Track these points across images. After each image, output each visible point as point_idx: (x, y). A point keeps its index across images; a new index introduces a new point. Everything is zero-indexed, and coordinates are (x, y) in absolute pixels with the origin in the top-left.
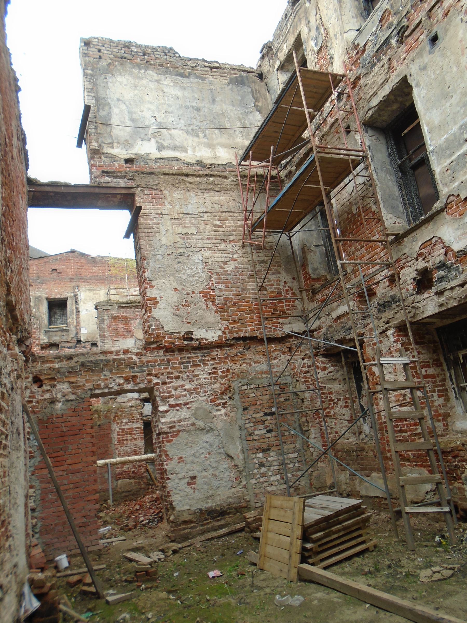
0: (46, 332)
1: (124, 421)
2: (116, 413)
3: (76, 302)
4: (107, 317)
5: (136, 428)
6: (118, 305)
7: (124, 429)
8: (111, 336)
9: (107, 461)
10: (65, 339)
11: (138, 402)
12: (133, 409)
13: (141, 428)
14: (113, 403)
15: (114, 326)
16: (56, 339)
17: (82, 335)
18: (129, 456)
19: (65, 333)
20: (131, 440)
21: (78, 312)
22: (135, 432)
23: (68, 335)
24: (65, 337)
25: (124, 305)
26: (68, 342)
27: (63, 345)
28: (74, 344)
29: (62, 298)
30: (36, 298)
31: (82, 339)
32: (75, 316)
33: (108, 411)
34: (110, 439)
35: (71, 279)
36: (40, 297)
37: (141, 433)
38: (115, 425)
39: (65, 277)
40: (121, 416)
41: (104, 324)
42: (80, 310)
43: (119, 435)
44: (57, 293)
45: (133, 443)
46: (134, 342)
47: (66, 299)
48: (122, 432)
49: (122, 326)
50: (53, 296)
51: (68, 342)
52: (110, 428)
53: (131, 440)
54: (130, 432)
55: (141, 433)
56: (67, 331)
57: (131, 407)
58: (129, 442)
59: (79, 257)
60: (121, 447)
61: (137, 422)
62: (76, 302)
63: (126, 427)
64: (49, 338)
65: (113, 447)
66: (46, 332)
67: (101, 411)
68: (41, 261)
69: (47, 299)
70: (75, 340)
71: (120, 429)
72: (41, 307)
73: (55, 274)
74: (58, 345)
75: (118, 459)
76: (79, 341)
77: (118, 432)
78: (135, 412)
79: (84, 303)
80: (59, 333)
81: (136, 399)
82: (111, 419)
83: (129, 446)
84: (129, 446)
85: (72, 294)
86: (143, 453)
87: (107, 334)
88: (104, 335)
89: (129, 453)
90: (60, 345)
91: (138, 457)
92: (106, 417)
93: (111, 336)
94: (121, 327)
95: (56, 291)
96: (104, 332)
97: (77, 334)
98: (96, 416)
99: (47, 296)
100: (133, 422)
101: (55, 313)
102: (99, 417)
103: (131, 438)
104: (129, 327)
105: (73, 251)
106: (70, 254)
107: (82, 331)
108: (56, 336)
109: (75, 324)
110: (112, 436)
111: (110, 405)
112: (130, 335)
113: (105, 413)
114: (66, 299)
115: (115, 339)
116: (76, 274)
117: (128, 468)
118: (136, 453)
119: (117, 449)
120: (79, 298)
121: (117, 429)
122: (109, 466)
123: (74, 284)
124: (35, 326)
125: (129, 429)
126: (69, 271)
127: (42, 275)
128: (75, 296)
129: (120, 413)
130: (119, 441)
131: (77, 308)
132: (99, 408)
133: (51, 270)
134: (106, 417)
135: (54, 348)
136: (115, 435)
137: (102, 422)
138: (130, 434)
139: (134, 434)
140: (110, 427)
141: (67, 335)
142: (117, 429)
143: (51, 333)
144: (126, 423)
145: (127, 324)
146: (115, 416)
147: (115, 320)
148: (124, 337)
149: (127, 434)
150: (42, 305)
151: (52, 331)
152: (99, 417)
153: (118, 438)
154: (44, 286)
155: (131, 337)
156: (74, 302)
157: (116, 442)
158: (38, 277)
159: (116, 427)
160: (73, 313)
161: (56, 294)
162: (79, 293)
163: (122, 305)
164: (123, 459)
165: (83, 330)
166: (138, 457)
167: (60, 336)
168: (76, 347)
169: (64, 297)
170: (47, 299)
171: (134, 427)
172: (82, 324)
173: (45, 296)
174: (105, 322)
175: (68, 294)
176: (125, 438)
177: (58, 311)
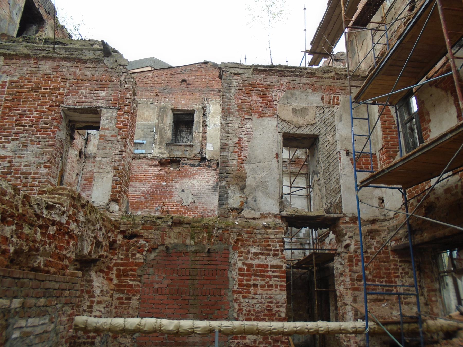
0: (167, 145)
1: (253, 250)
2: (240, 235)
3: (204, 115)
4: (235, 84)
5: (272, 266)
6: (253, 68)
7: (251, 266)
8: (240, 111)
9: (215, 324)
10: (188, 154)
11: (279, 221)
12: (269, 231)
13: (281, 267)
14: (235, 218)
15: (245, 97)
16: (178, 153)
17: (207, 152)
18: (257, 319)
19: (188, 148)
20: (262, 287)
21: (205, 126)
22: (270, 273)
23: (191, 151)
24: (187, 153)
25: (263, 68)
26: (191, 159)
27: (184, 162)
28: (197, 162)
29: (189, 111)
30: (161, 109)
31: (207, 157)
32: (201, 131)
33: (226, 230)
34: (226, 282)
35: (201, 91)
36: (165, 107)
37: (281, 277)
38: (236, 255)
39: (194, 88)
40: (247, 241)
41: (230, 93)
42: (208, 124)
43: (243, 275)
44: (184, 104)
45: (266, 293)
46: (275, 124)
47: (194, 111)
48: (248, 270)
49: (259, 99)
50: (180, 107)
51: (191, 159)
52: (226, 260)
53: (262, 287)
54: (262, 271)
55: (281, 277)
56: (191, 146)
57: (266, 227)
58: (260, 291)
59: (212, 69)
60: (244, 297)
61: (275, 255)
62: (204, 115)
63: (256, 262)
64: (170, 152)
65: (230, 296)
66: (167, 145)
67: (214, 227)
68: (171, 71)
69: (173, 110)
70: (199, 157)
71: (243, 264)
72: (165, 119)
73: (184, 85)
74: (179, 161)
75: (237, 324)
76: (203, 159)
77: (240, 269)
78: (272, 237)
79: (213, 117)
80: (182, 148)
81: (275, 216)
82: (229, 244)
83: (258, 299)
84: (258, 299)
85: (201, 107)
86: (283, 315)
87: (234, 108)
88: (229, 110)
89: (257, 312)
90: (182, 161)
91: (276, 325)
92: (221, 239)
93: (240, 111)
94: (256, 100)
95: (184, 102)
96: (229, 105)
97: (202, 150)
98: (205, 235)
99: (173, 107)
100: (269, 255)
101: (182, 131)
102: (209, 238)
103: (263, 283)
104: (270, 101)
105: (206, 63)
106: (202, 66)
107: (208, 148)
108: (178, 150)
109: (201, 138)
110: (230, 275)
111: (230, 220)
112: (270, 113)
113: (221, 231)
114: (194, 111)
115: (246, 117)
116: (207, 86)
117: (255, 341)
118: (270, 315)
119: (236, 300)
120: (208, 110)
121: (239, 264)
122: (217, 334)
123: (203, 96)
124: (127, 86)
125: (259, 266)
126: (199, 82)
127: (170, 85)
128: (204, 108)
129: (246, 236)
130: (241, 285)
131: (204, 122)
132: (211, 223)
133: (180, 81)
134: (221, 239)
135: (175, 165)
136: (235, 274)
137: (214, 247)
138: (262, 276)
139: (269, 277)
140: (227, 258)
141: (190, 150)
142: (239, 264)
143: (173, 147)
144: (256, 254)
145: (266, 98)
146: (238, 240)
147: (247, 88)
148: (261, 115)
149: (256, 275)
150: (167, 115)
151: (174, 145)
152: (209, 238)
153: (241, 281)
154: (171, 96)
155: (271, 116)
156: (202, 115)
157: (236, 288)
158: (166, 87)
159: (237, 260)
160: (200, 127)
161: (183, 105)
162: (208, 106)
163: (259, 68)
164: (248, 324)
165: (209, 147)
166: (276, 325)
167: (182, 152)
168: (199, 165)
169: (191, 109)
170: (173, 110)
171: (269, 264)
172: (208, 139)
173: (171, 106)
174: (233, 91)
175: (196, 106)
176: (252, 282)
177: (185, 129)
